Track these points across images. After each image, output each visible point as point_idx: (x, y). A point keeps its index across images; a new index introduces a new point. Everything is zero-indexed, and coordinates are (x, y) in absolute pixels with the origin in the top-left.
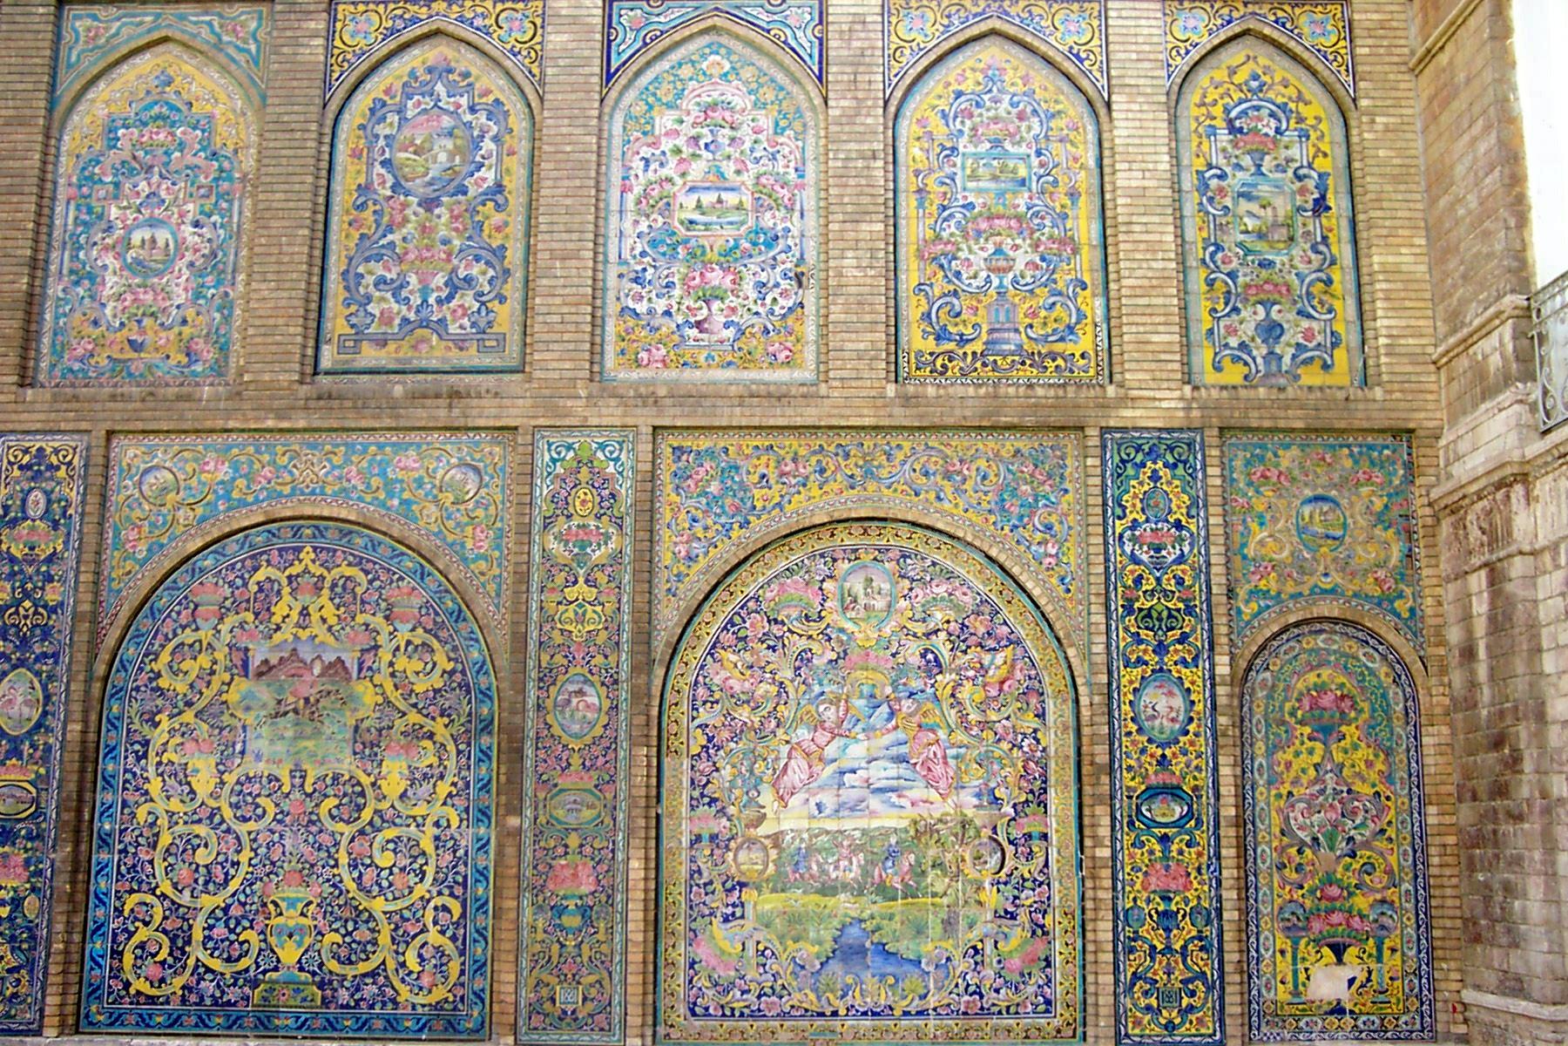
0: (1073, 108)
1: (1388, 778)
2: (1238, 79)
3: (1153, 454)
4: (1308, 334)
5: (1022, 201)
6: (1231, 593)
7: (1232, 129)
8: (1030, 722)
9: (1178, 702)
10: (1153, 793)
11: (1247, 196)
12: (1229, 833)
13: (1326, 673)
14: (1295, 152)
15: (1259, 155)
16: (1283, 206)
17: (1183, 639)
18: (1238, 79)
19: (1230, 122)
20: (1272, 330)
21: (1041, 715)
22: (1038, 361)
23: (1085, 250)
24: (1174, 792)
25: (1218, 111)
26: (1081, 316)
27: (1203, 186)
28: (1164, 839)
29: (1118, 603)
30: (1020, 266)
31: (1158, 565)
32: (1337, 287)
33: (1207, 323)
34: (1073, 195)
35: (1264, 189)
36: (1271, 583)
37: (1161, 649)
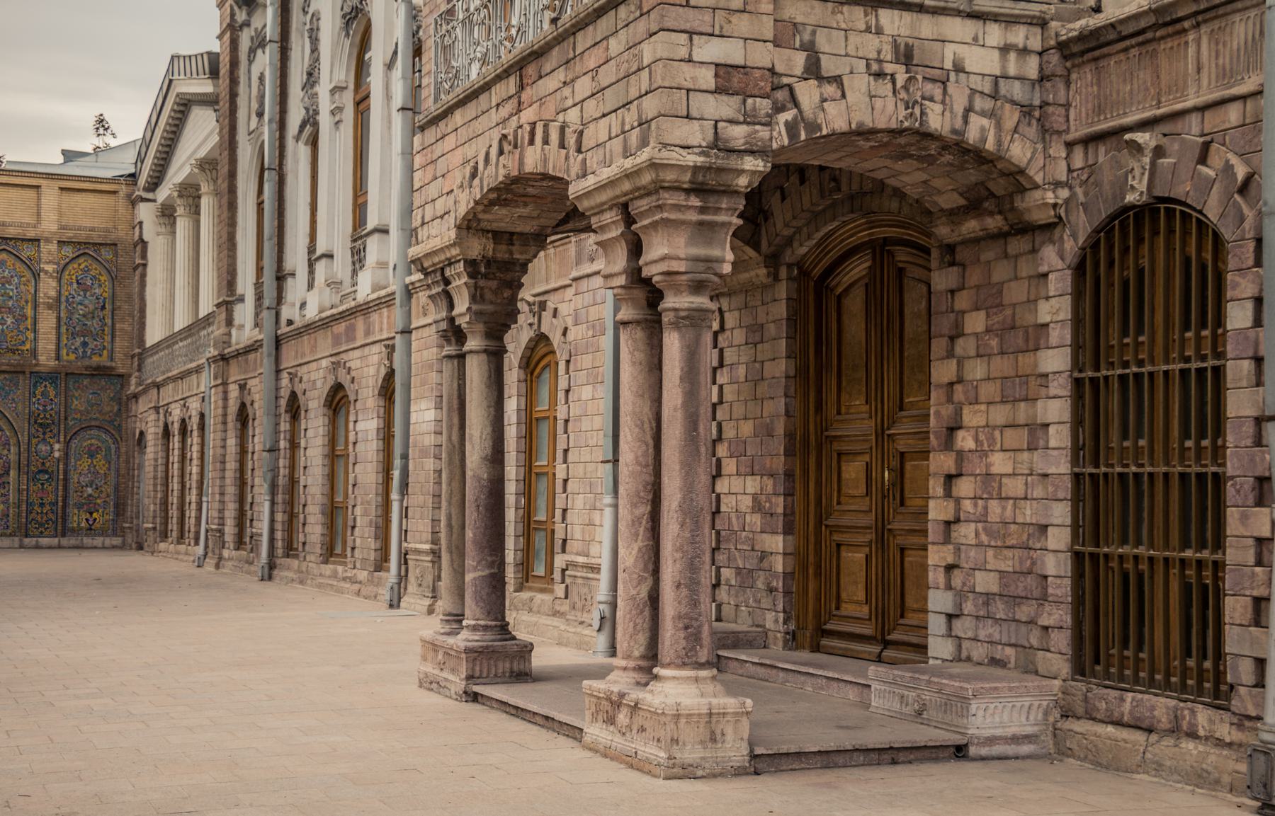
0: (28, 274)
1: (109, 469)
2: (81, 267)
3: (45, 380)
4: (96, 346)
5: (10, 303)
6: (66, 419)
7: (78, 282)
8: (5, 452)
9: (49, 448)
10: (40, 472)
11: (81, 304)
12: (61, 483)
13: (93, 441)
14: (97, 291)
15: (85, 291)
16: (91, 307)
17: (51, 431)
18: (81, 267)
19: (77, 281)
20: (85, 344)
21: (9, 450)
22: (13, 351)
23: (29, 320)
24: (46, 472)
25: (74, 277)
26: (27, 338)
27: (67, 301)
28: (42, 484)
29: (32, 421)
30: (9, 323)
31: (45, 410)
32: (106, 332)
33: (65, 342)
34: (27, 302)
35: (86, 302)
36: (78, 416)
37: (44, 433)
